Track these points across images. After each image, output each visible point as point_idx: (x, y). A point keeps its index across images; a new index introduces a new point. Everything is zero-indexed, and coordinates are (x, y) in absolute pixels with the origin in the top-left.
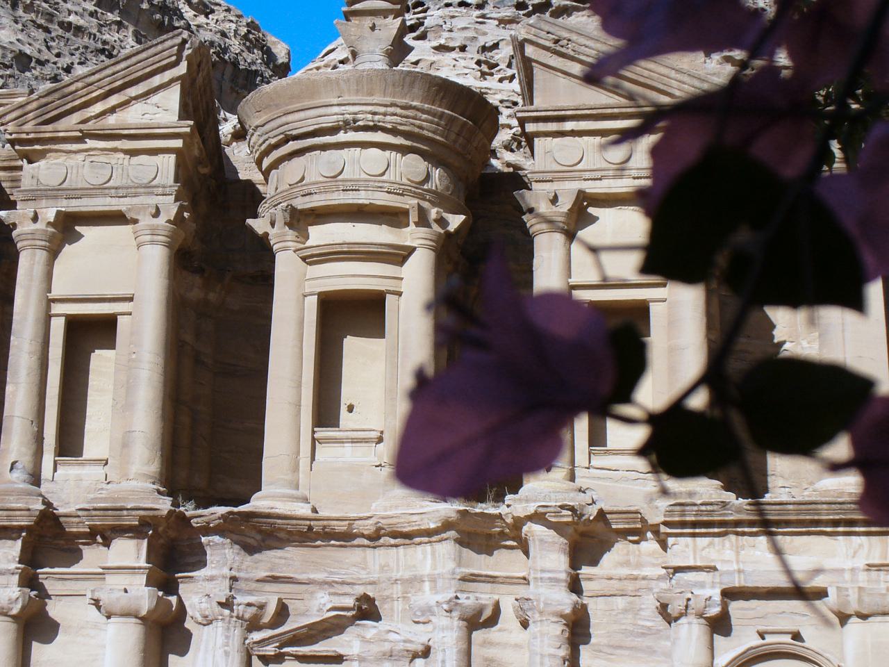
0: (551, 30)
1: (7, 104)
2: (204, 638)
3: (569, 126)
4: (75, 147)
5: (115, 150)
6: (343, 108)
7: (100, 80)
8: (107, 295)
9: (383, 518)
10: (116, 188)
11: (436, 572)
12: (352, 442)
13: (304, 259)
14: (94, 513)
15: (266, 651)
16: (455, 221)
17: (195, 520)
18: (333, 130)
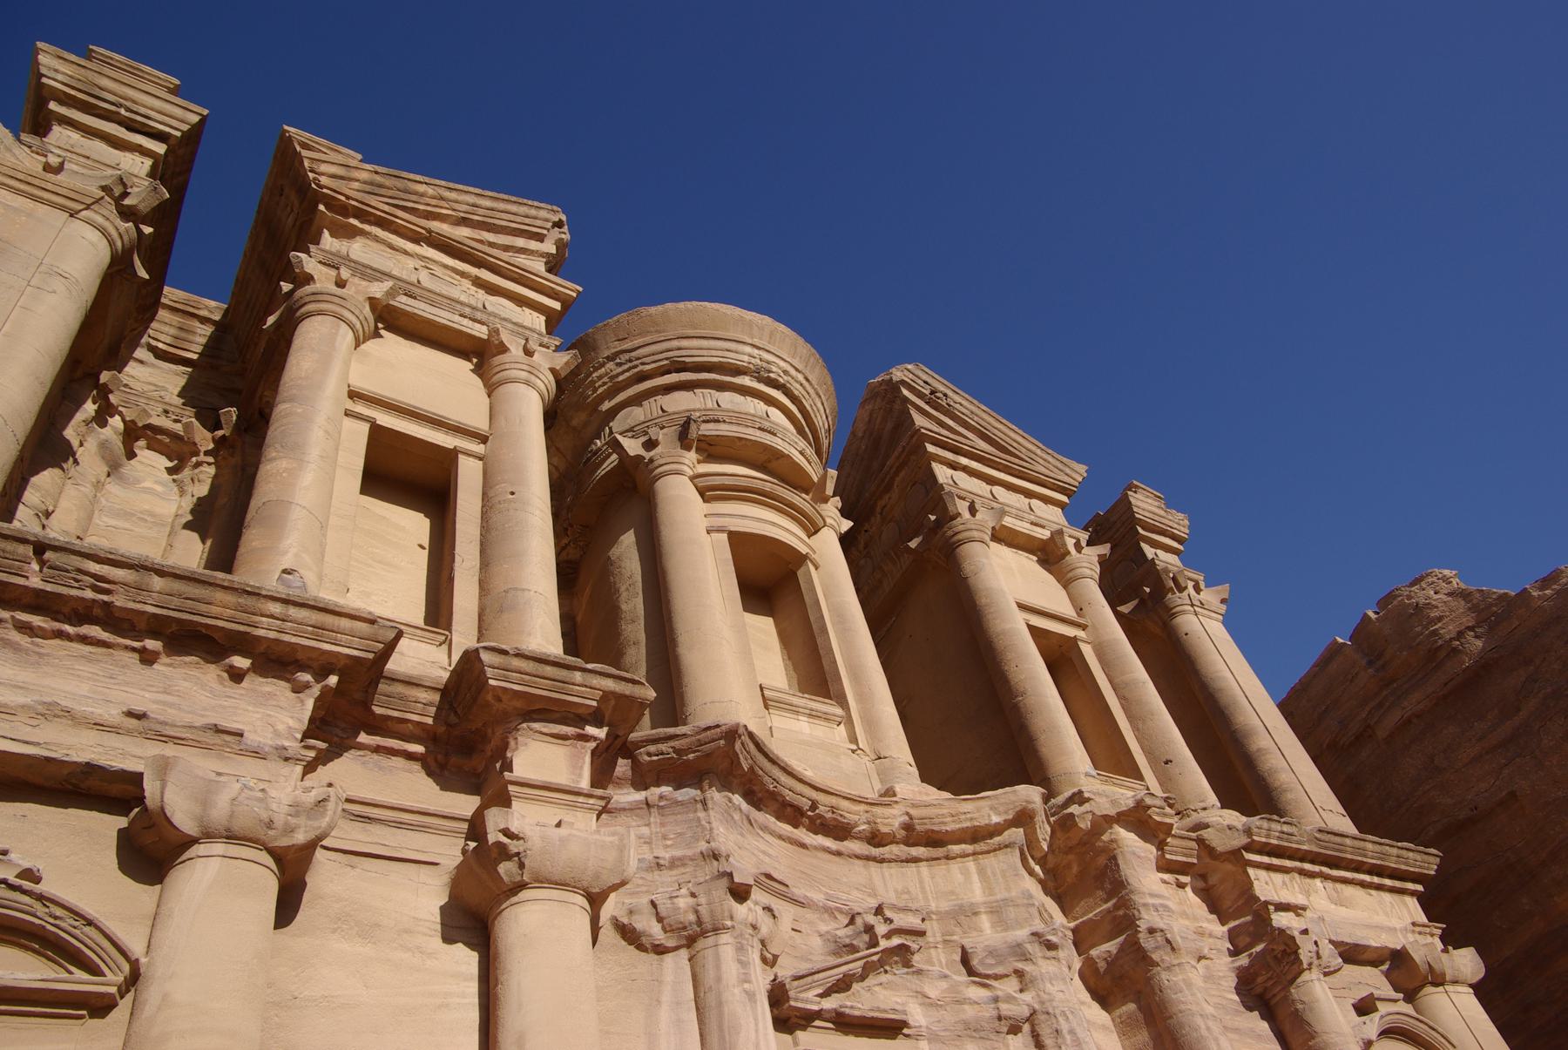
0: (930, 380)
1: (325, 153)
2: (669, 977)
3: (964, 461)
4: (409, 246)
5: (463, 274)
6: (756, 352)
7: (456, 202)
8: (449, 419)
9: (914, 806)
10: (473, 308)
11: (999, 897)
12: (810, 716)
13: (702, 492)
14: (517, 663)
15: (802, 1001)
16: (846, 525)
17: (652, 748)
18: (738, 371)
